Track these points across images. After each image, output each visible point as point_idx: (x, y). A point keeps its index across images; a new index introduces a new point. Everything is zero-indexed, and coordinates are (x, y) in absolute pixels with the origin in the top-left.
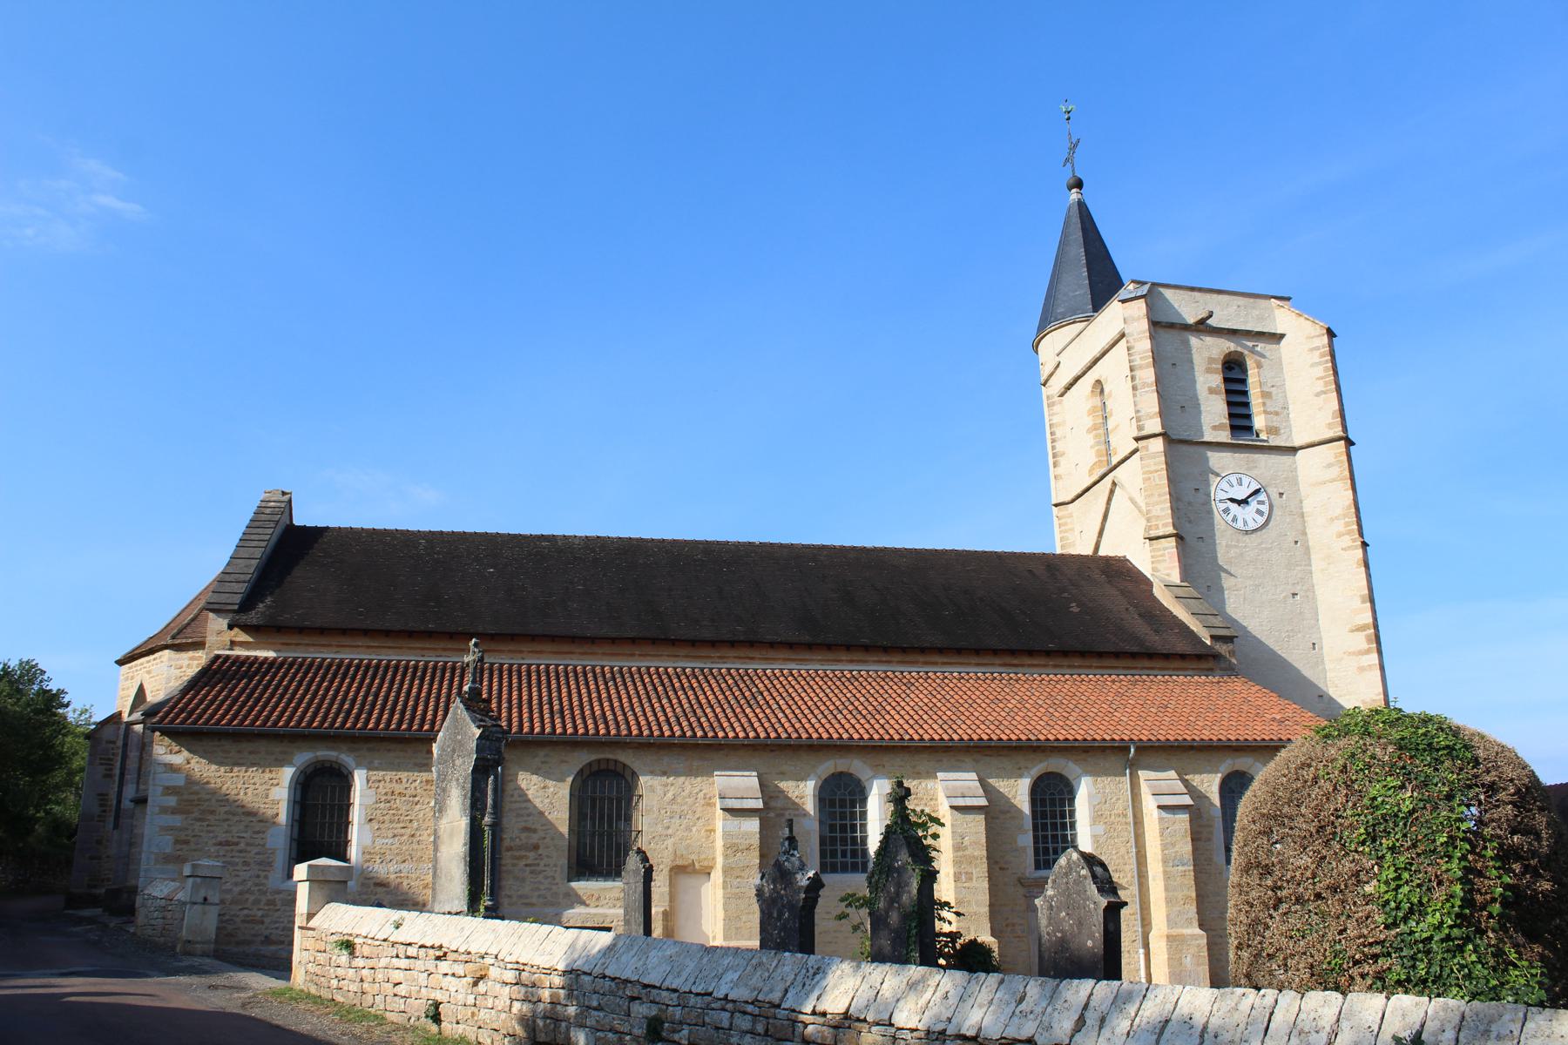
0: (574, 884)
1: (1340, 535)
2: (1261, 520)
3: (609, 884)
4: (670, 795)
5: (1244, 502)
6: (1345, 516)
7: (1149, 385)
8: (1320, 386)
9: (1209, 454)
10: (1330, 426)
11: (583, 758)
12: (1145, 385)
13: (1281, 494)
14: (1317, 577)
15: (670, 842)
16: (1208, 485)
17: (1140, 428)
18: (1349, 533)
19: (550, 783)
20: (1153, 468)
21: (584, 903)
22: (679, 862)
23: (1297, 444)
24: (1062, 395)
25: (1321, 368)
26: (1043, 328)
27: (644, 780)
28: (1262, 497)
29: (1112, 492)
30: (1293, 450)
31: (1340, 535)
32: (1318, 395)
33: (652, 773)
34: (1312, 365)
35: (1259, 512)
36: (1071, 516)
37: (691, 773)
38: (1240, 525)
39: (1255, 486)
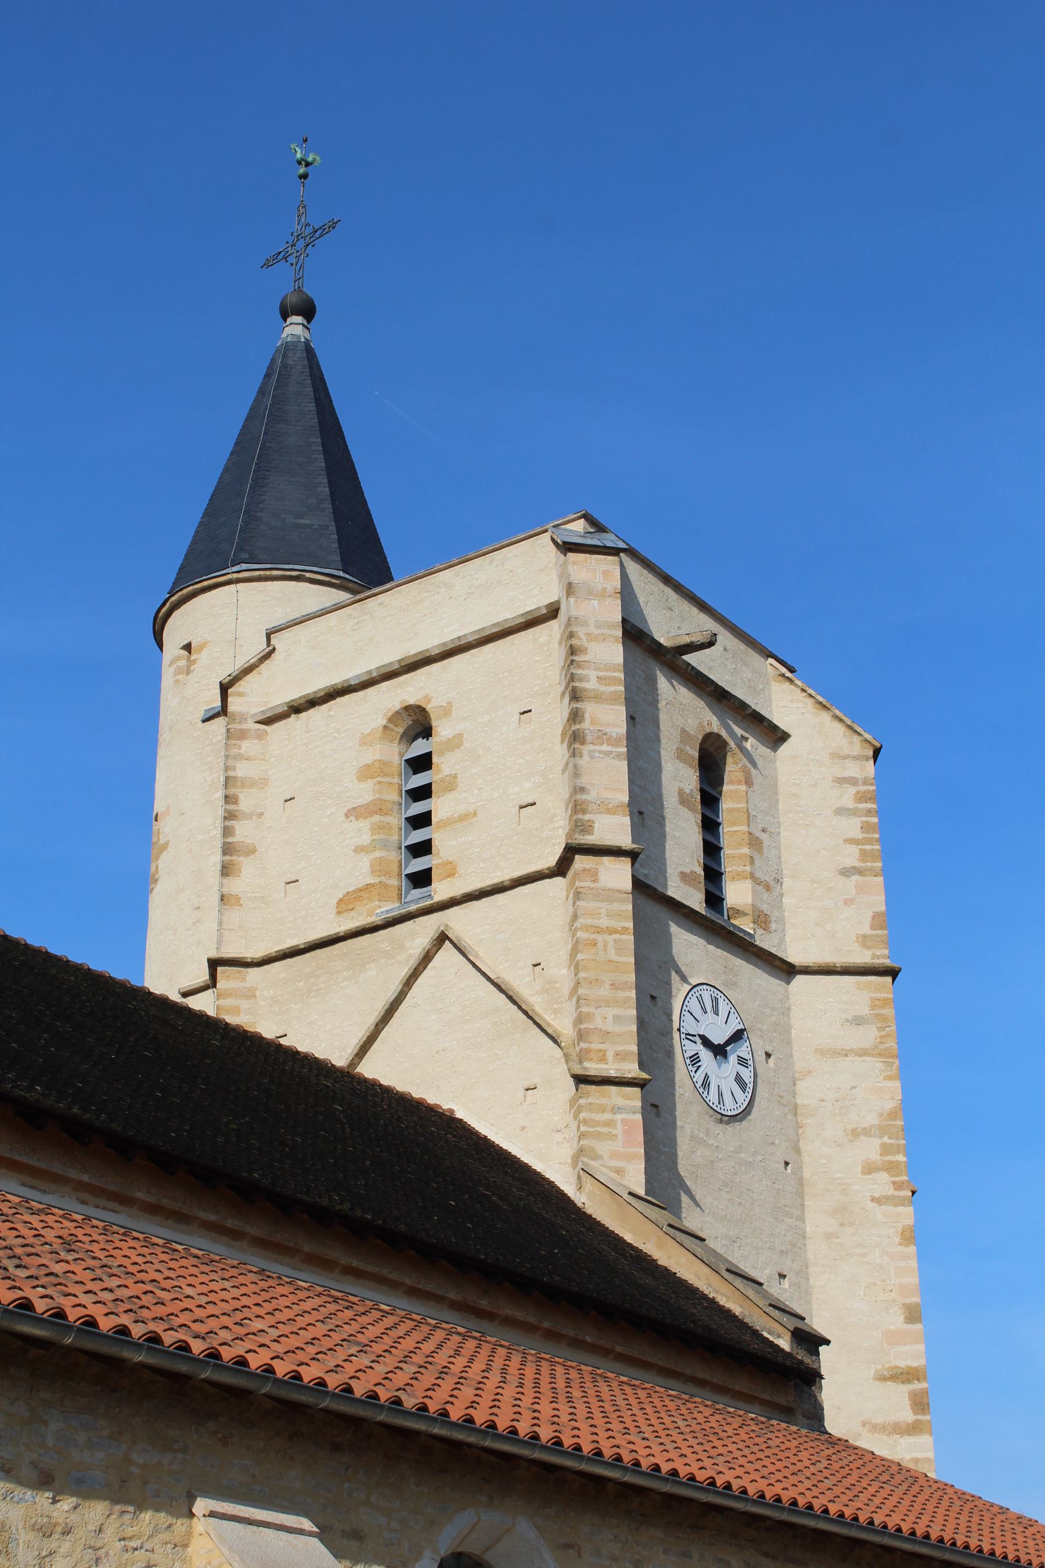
1: (870, 1169)
2: (743, 1099)
6: (883, 1131)
7: (610, 741)
8: (851, 857)
9: (674, 928)
10: (865, 941)
12: (602, 737)
13: (768, 1055)
14: (815, 1249)
16: (669, 995)
17: (580, 827)
18: (891, 1168)
20: (604, 922)
23: (795, 957)
24: (269, 721)
26: (206, 563)
28: (743, 1050)
29: (427, 958)
30: (788, 970)
31: (870, 1169)
32: (846, 872)
34: (840, 811)
35: (739, 1079)
36: (250, 994)
37: (127, 1490)
39: (734, 1026)
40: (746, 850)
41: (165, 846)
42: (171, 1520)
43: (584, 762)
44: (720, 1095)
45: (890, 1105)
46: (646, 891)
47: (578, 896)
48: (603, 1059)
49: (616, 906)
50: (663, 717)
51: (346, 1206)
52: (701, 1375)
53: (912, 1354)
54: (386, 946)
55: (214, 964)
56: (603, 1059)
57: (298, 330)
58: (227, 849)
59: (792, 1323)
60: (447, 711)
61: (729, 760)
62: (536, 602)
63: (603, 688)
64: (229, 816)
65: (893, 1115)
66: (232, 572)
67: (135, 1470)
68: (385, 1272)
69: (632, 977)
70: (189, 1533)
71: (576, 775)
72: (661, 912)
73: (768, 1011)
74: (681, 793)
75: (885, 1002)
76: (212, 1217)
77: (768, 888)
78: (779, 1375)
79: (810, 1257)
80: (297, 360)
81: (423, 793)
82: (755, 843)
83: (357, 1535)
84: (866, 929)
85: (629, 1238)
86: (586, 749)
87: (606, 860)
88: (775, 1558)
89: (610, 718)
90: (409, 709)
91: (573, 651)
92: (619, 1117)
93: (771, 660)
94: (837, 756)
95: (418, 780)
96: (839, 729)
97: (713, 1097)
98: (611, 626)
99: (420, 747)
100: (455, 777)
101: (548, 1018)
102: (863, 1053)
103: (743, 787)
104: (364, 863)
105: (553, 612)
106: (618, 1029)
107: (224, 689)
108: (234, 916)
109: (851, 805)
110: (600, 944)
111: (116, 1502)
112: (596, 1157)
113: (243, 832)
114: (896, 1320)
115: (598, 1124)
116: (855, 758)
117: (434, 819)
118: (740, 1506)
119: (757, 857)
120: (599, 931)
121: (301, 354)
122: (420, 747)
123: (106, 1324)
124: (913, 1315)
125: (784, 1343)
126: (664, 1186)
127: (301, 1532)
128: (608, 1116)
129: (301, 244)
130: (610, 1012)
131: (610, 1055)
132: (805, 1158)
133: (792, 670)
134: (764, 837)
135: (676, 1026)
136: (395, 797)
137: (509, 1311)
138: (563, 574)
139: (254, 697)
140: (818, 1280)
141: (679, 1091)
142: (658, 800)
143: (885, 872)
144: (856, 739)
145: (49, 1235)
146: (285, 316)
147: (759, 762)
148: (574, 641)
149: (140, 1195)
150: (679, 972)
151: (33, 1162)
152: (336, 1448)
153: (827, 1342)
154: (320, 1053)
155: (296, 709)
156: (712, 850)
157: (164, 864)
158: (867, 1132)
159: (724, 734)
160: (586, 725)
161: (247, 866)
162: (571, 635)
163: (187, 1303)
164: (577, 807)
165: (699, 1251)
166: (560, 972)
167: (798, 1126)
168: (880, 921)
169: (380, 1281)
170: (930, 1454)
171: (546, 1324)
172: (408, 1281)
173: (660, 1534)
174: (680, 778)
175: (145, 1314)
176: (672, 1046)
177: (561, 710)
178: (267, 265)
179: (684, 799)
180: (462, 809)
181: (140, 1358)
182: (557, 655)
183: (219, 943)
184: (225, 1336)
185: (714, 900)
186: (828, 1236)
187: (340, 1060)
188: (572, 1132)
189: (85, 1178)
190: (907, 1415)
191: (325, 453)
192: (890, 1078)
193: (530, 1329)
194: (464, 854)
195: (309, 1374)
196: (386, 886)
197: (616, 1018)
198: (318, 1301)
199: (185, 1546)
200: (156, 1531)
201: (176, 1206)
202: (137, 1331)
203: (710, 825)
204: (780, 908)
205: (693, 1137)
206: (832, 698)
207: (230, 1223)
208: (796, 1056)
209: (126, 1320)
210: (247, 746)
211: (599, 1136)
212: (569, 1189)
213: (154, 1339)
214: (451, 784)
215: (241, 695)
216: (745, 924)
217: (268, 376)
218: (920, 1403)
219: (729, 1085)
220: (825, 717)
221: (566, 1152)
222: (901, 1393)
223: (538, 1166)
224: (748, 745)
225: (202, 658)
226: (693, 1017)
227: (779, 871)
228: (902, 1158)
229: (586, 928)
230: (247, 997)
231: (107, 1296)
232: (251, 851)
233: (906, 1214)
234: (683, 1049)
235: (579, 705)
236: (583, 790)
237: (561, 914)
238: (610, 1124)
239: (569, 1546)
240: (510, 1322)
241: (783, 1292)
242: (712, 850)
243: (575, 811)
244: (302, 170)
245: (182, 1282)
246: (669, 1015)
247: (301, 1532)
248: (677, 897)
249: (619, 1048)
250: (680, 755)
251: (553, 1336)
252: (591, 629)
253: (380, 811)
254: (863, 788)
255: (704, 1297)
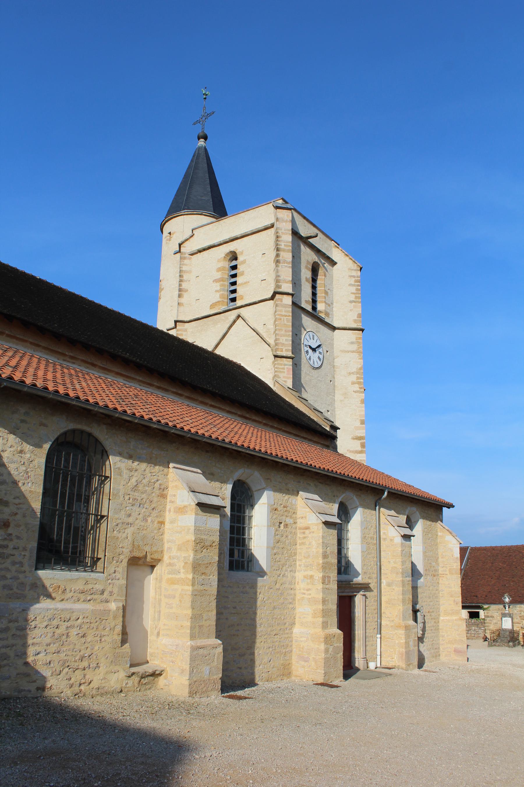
0: (41, 573)
1: (353, 383)
2: (320, 363)
3: (74, 574)
4: (133, 481)
5: (314, 350)
6: (357, 373)
7: (287, 263)
9: (303, 316)
10: (355, 321)
11: (61, 425)
12: (285, 262)
13: (327, 351)
14: (337, 404)
15: (130, 531)
16: (301, 334)
18: (359, 383)
19: (27, 447)
20: (284, 313)
21: (49, 596)
22: (137, 554)
23: (336, 325)
24: (192, 254)
25: (355, 288)
27: (116, 465)
28: (321, 350)
29: (234, 322)
30: (334, 329)
31: (353, 383)
32: (351, 302)
33: (120, 454)
34: (350, 285)
35: (319, 358)
36: (186, 330)
37: (152, 460)
38: (311, 363)
40: (324, 295)
41: (163, 289)
42: (163, 468)
43: (280, 268)
44: (314, 362)
45: (360, 366)
46: (295, 305)
47: (277, 306)
48: (282, 351)
49: (287, 309)
50: (302, 257)
51: (211, 389)
52: (305, 436)
53: (362, 433)
54: (223, 318)
55: (176, 322)
56: (282, 351)
57: (203, 143)
58: (180, 290)
59: (330, 424)
60: (242, 253)
61: (320, 269)
62: (268, 223)
63: (286, 248)
64: (181, 281)
65: (360, 369)
66: (182, 212)
67: (154, 455)
68: (221, 406)
69: (291, 329)
70: (168, 472)
71: (277, 272)
72: (300, 311)
73: (328, 339)
74: (306, 278)
75: (360, 338)
76: (175, 390)
77: (329, 305)
78: (326, 437)
79: (336, 406)
80: (202, 152)
81: (234, 276)
82: (326, 293)
83: (212, 474)
84: (356, 318)
85: (287, 399)
86: (280, 265)
87: (285, 296)
88: (322, 483)
89: (287, 256)
90: (231, 252)
91: (277, 237)
92: (286, 367)
93: (333, 242)
94: (350, 269)
95: (233, 272)
96: (351, 262)
97: (311, 363)
98: (288, 230)
99: (234, 263)
100: (243, 272)
101: (267, 339)
102: (353, 352)
103: (324, 277)
104: (218, 295)
105: (272, 226)
106: (286, 343)
107: (180, 245)
108: (181, 309)
109: (353, 283)
110: (282, 319)
111: (149, 463)
112: (279, 378)
113: (184, 285)
114: (358, 424)
115: (280, 368)
116: (355, 270)
117: (237, 283)
118: (314, 470)
119: (326, 297)
120: (282, 316)
121: (203, 150)
122: (234, 263)
123: (146, 417)
124: (362, 422)
125: (328, 429)
126: (297, 386)
127: (197, 473)
128: (283, 367)
129: (204, 118)
130: (284, 338)
131: (284, 350)
132: (336, 380)
133: (339, 245)
134: (329, 291)
135: (302, 342)
136: (227, 277)
137: (254, 418)
138: (276, 215)
139: (188, 248)
140: (337, 412)
141: (302, 360)
142: (300, 280)
143: (362, 302)
144: (355, 265)
145: (131, 393)
146: (199, 139)
147: (328, 270)
148: (278, 234)
149: (155, 384)
150: (304, 328)
151: (126, 374)
152: (207, 452)
153: (339, 429)
154: (205, 347)
155: (200, 251)
156: (314, 294)
157: (162, 294)
158: (353, 373)
159: (319, 262)
160: (280, 258)
161: (185, 295)
162: (277, 233)
163: (168, 413)
164: (277, 281)
165: (306, 404)
166: (271, 327)
167: (334, 371)
168: (359, 316)
169: (220, 408)
170: (365, 459)
171: (264, 422)
172: (227, 409)
173: (292, 477)
174: (306, 274)
175: (156, 415)
176: (301, 348)
177: (274, 253)
178: (194, 124)
179: (307, 280)
180: (245, 280)
181: (155, 426)
182: (273, 238)
183: (177, 316)
184: (178, 421)
185: (314, 308)
186: (341, 401)
187: (210, 349)
188: (273, 371)
189: (141, 379)
190: (359, 448)
191: (210, 178)
192: (360, 359)
193: (260, 423)
194: (245, 294)
195: (200, 432)
196: (224, 301)
197: (286, 340)
198: (203, 413)
199: (167, 475)
200: (159, 471)
201: (165, 387)
202: (155, 419)
203: (314, 287)
204: (332, 311)
205: (306, 373)
206: (350, 253)
207: (179, 392)
208: (335, 352)
209: (151, 416)
210: (186, 261)
211: (280, 372)
212: (272, 386)
213: (159, 421)
214: (242, 274)
215: (184, 247)
216: (323, 315)
217: (194, 156)
218: (363, 445)
219: (316, 359)
220: (347, 258)
221: (271, 376)
222: (358, 442)
223: (263, 379)
224: (325, 265)
225: (174, 236)
226: (308, 340)
227: (332, 301)
228: (362, 381)
229: (278, 315)
230: (185, 331)
231: (146, 410)
232: (186, 291)
233: (362, 396)
234: (304, 349)
235: (279, 252)
236: (279, 276)
237: (272, 311)
238: (283, 369)
239: (268, 479)
240: (254, 421)
241: (328, 415)
242: (314, 294)
243: (277, 282)
244: (205, 97)
245: (166, 407)
246: (301, 340)
247: (197, 473)
248: (304, 307)
249: (287, 348)
250: (306, 267)
251: (265, 425)
252: (283, 231)
253: (223, 281)
254: (357, 279)
255: (307, 416)
